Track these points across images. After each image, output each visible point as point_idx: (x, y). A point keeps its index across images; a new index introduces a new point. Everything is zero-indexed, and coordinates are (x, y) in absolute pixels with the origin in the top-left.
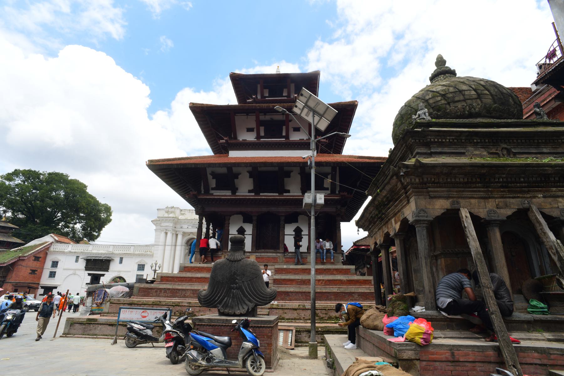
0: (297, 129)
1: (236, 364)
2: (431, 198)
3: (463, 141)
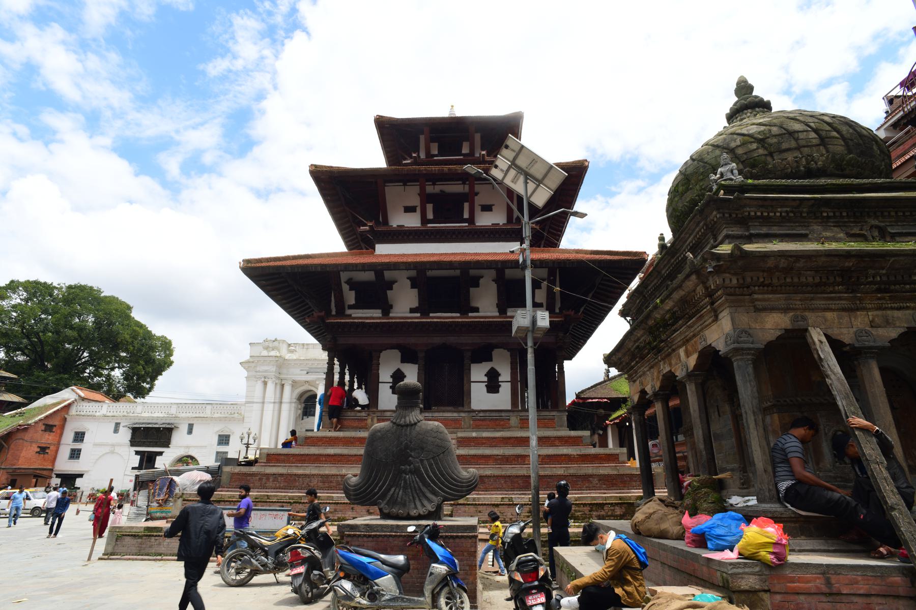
0: (487, 208)
1: (421, 603)
2: (757, 310)
3: (805, 215)
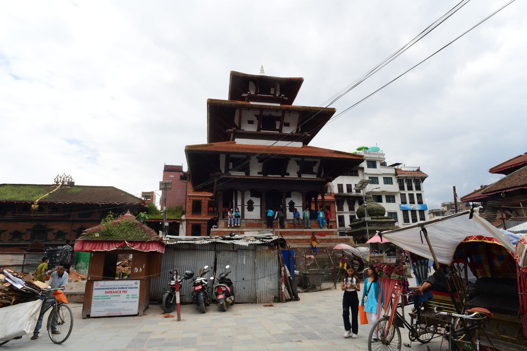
0: (287, 125)
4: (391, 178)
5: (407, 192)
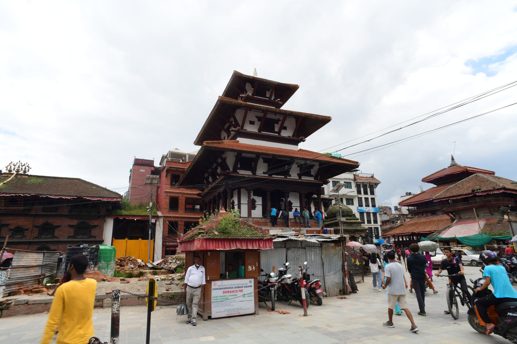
4: (351, 183)
5: (363, 196)
